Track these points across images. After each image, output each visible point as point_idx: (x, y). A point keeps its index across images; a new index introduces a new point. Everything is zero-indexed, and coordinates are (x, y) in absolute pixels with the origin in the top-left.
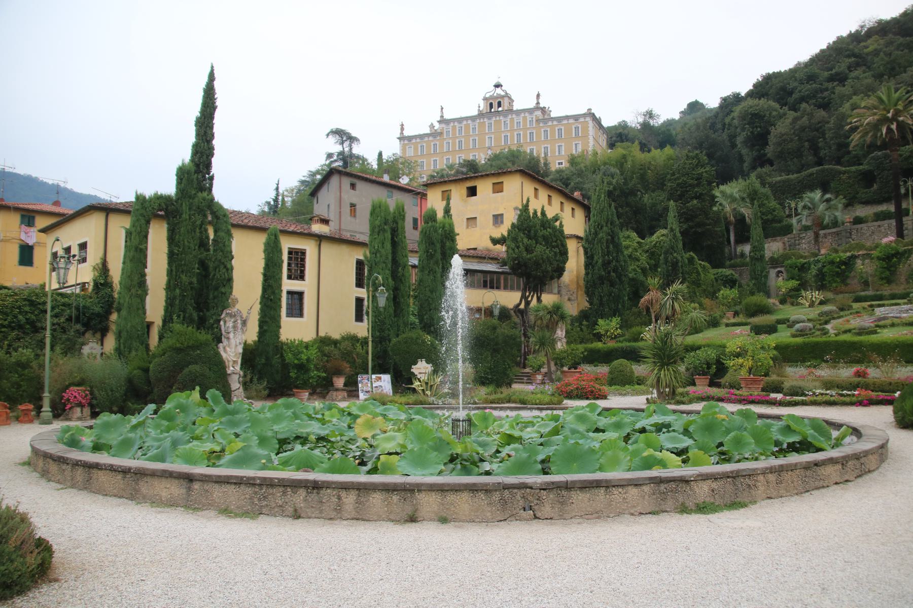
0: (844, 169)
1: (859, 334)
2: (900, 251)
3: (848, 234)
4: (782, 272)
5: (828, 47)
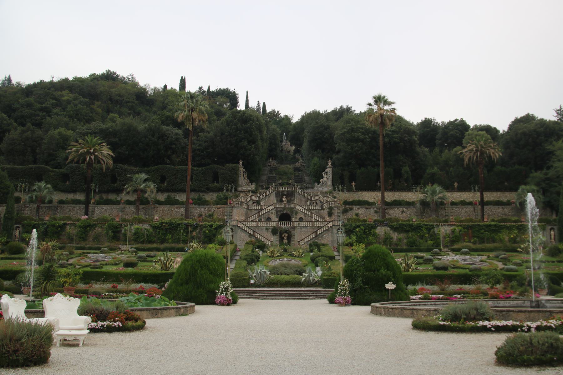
0: (52, 169)
1: (94, 268)
2: (92, 224)
3: (56, 209)
4: (19, 227)
5: (33, 84)
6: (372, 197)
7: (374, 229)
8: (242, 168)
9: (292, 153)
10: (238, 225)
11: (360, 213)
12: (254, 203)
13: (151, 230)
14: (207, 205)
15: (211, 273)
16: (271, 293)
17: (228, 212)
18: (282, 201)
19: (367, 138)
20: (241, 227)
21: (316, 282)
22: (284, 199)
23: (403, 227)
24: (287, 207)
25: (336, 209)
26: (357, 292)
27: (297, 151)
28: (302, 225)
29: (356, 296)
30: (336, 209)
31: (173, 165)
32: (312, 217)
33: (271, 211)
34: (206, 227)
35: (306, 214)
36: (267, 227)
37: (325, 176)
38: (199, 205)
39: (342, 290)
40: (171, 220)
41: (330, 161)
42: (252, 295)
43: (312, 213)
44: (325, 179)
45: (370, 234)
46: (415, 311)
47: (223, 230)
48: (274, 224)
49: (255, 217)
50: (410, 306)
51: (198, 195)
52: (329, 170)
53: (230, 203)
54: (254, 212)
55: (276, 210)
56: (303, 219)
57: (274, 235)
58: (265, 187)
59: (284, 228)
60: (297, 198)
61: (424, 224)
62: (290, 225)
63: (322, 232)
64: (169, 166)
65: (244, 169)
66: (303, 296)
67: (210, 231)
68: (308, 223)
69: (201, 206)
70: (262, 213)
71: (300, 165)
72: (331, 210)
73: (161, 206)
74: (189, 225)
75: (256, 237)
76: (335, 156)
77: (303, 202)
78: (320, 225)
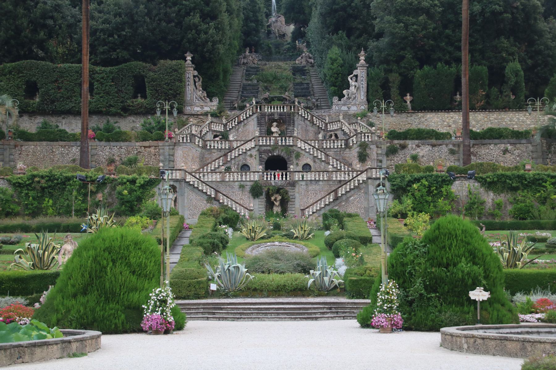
6: (446, 123)
7: (448, 185)
8: (192, 69)
9: (289, 38)
10: (185, 180)
11: (421, 154)
12: (215, 136)
13: (10, 190)
14: (125, 140)
15: (134, 273)
16: (249, 309)
17: (167, 154)
18: (270, 133)
19: (436, 5)
20: (191, 183)
21: (336, 287)
22: (274, 129)
23: (505, 181)
24: (280, 144)
25: (373, 147)
26: (414, 305)
27: (298, 35)
28: (309, 179)
29: (413, 313)
30: (373, 147)
31: (52, 61)
32: (329, 163)
33: (249, 153)
34: (123, 184)
35: (317, 156)
36: (242, 183)
37: (352, 83)
38: (108, 140)
39: (383, 301)
40: (51, 171)
41: (362, 53)
42: (214, 314)
43: (327, 155)
44: (352, 89)
45: (440, 194)
46: (528, 345)
47: (156, 190)
48: (254, 176)
49: (219, 163)
50: (518, 333)
51: (105, 121)
52: (361, 72)
53: (170, 138)
54: (215, 155)
55: (258, 150)
56: (309, 165)
57: (254, 198)
58: (236, 105)
59: (273, 184)
60: (300, 127)
61: (548, 176)
62: (286, 178)
63: (347, 192)
64: (43, 63)
65: (194, 69)
66: (311, 313)
67: (131, 192)
68: (319, 175)
69: (112, 144)
70: (231, 156)
71: (304, 63)
72: (365, 150)
73: (30, 143)
74: (89, 179)
75: (221, 201)
76: (372, 44)
77: (311, 135)
78: (343, 179)
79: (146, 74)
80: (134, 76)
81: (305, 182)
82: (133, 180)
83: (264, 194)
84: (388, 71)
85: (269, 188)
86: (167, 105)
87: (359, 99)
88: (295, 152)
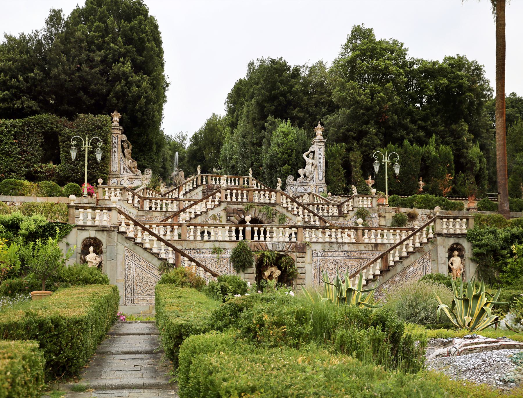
36: (217, 245)
44: (308, 167)
55: (225, 209)
59: (270, 248)
79: (61, 131)
80: (43, 133)
81: (321, 245)
82: (13, 222)
83: (254, 264)
84: (349, 150)
85: (264, 254)
86: (87, 143)
87: (317, 179)
88: (278, 215)
